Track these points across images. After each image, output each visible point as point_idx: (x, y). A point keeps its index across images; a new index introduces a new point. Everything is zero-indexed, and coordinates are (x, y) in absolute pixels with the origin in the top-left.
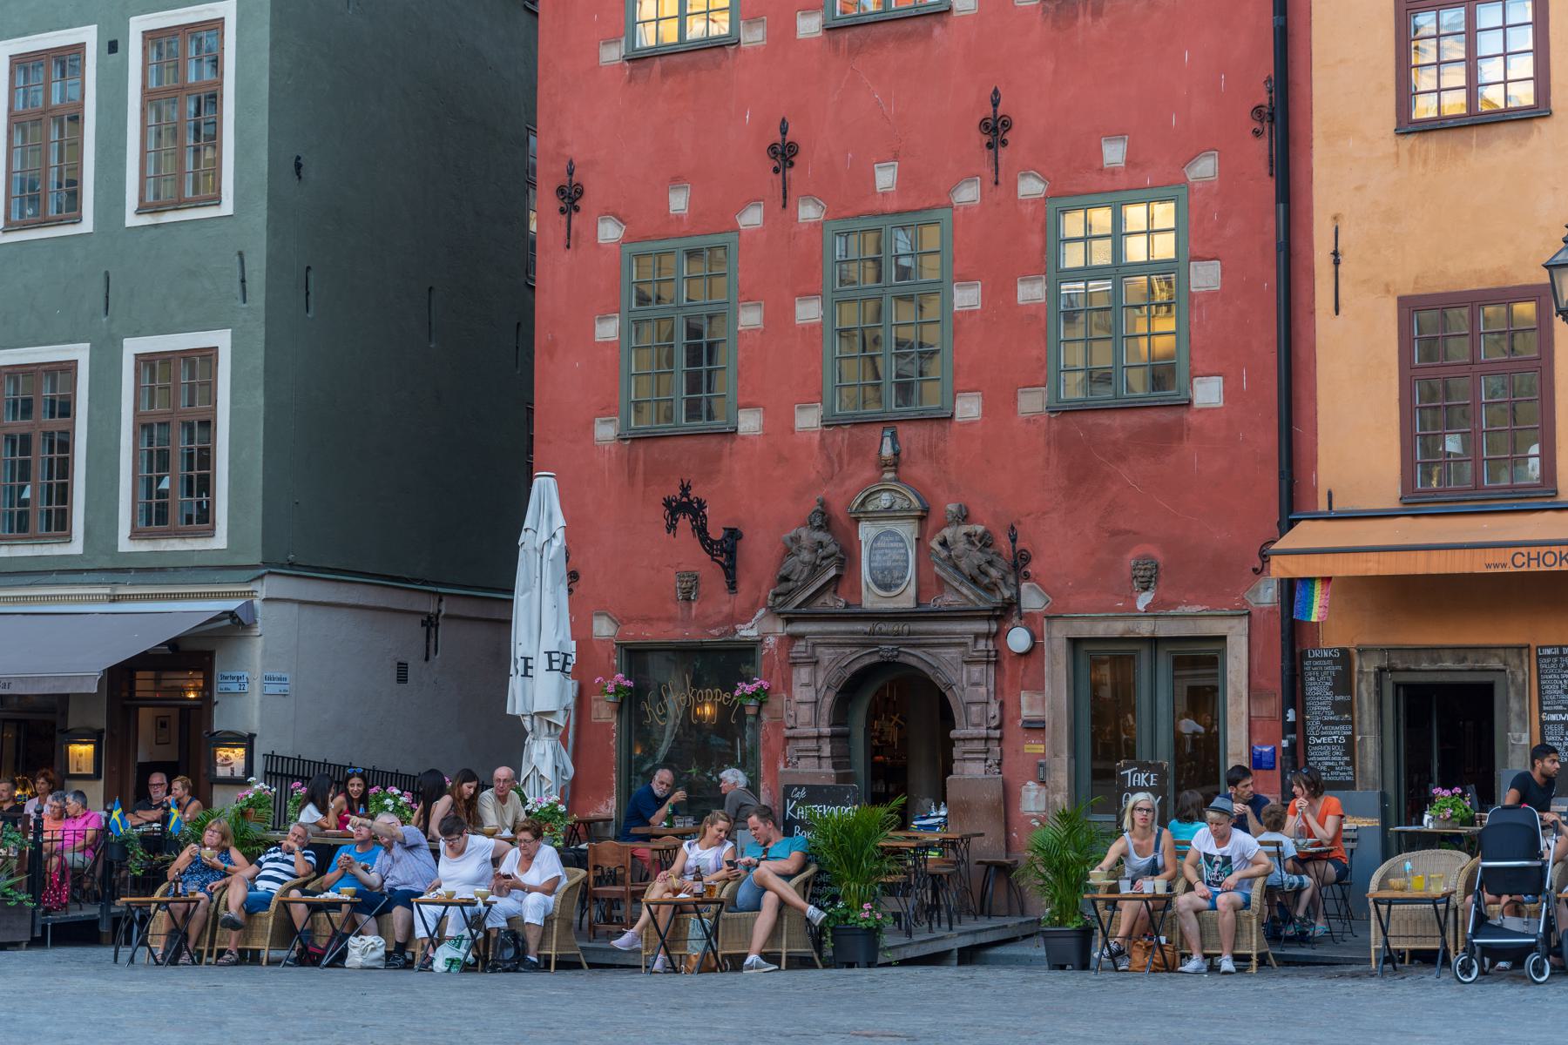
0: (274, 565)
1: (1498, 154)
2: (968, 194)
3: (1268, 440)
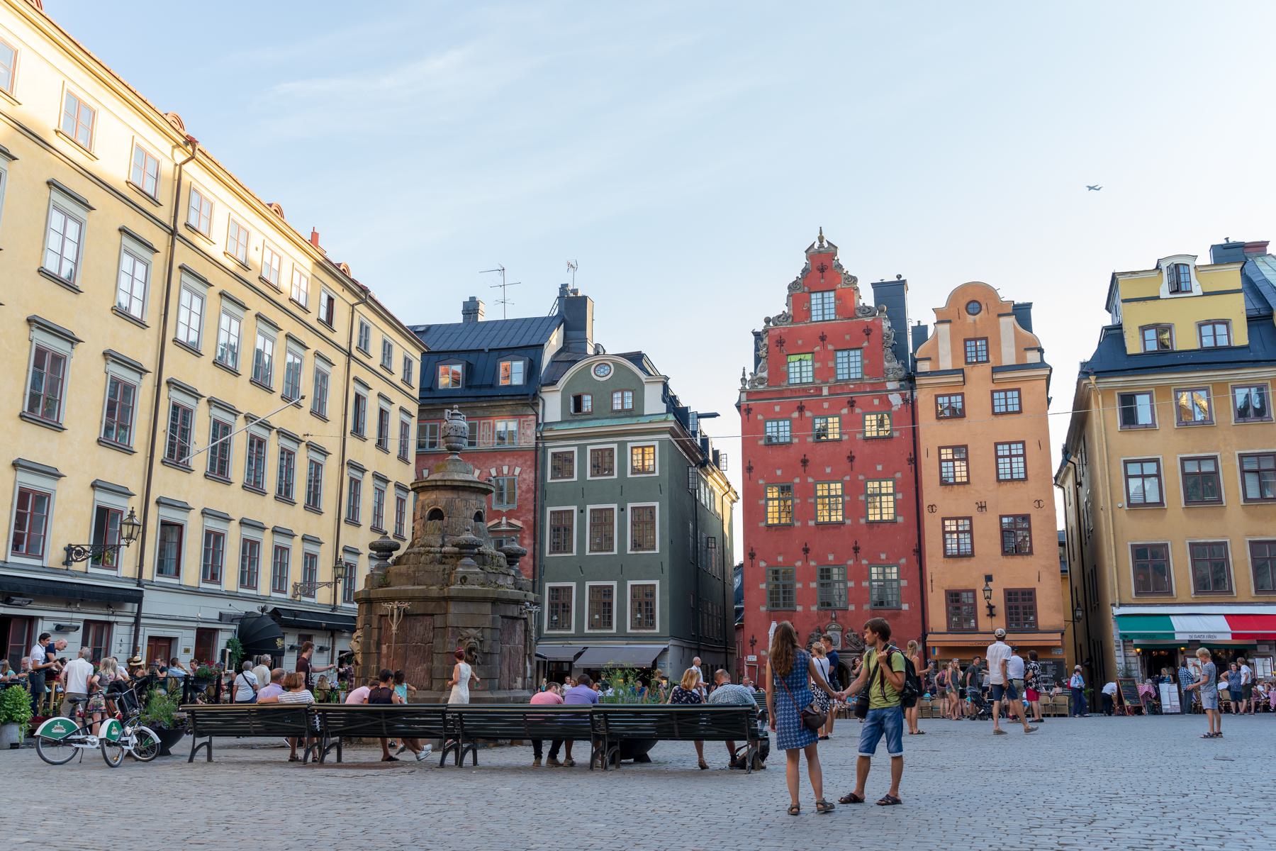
0: (673, 637)
1: (964, 563)
2: (850, 562)
3: (919, 617)
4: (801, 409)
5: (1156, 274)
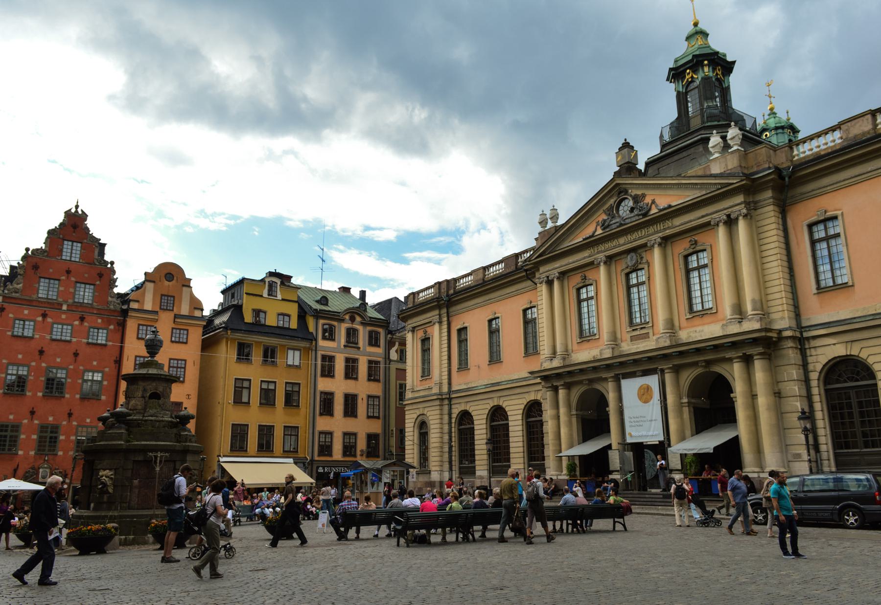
2: (64, 423)
4: (44, 316)
5: (262, 284)
